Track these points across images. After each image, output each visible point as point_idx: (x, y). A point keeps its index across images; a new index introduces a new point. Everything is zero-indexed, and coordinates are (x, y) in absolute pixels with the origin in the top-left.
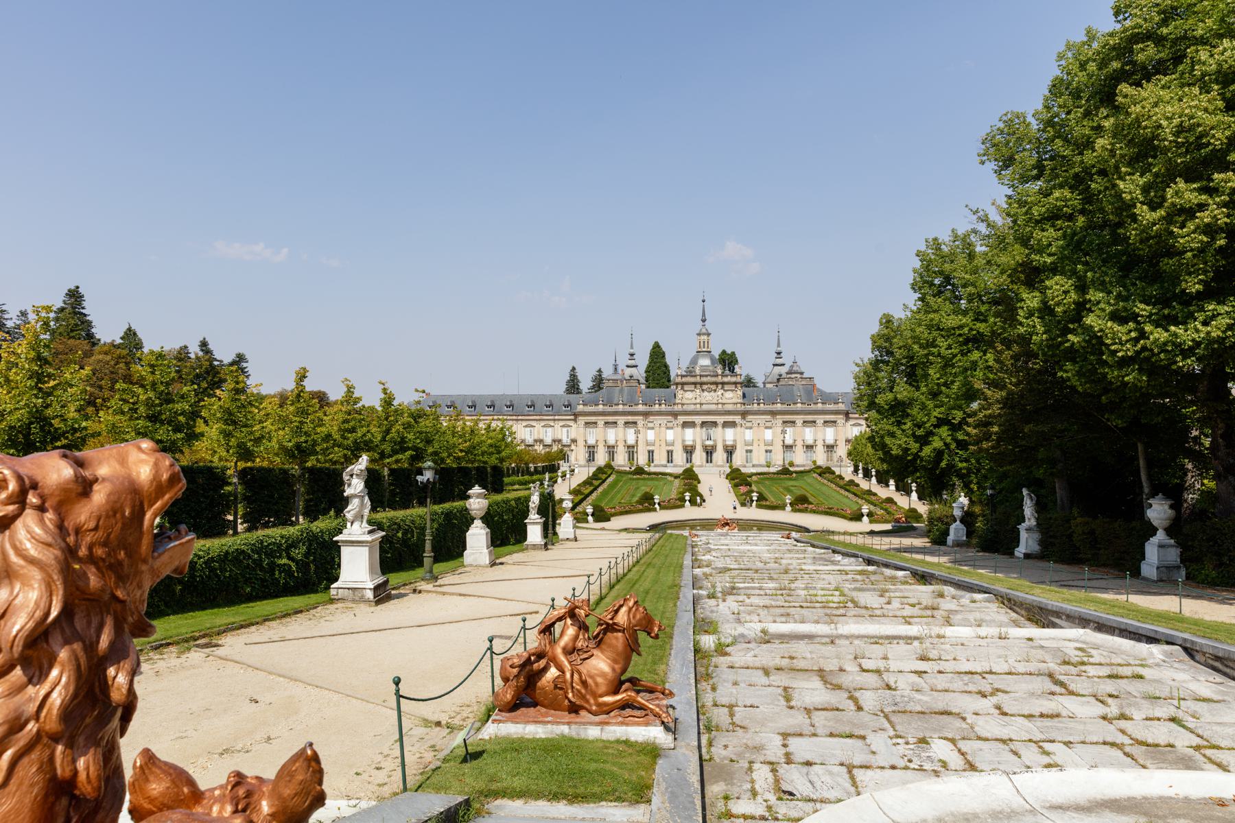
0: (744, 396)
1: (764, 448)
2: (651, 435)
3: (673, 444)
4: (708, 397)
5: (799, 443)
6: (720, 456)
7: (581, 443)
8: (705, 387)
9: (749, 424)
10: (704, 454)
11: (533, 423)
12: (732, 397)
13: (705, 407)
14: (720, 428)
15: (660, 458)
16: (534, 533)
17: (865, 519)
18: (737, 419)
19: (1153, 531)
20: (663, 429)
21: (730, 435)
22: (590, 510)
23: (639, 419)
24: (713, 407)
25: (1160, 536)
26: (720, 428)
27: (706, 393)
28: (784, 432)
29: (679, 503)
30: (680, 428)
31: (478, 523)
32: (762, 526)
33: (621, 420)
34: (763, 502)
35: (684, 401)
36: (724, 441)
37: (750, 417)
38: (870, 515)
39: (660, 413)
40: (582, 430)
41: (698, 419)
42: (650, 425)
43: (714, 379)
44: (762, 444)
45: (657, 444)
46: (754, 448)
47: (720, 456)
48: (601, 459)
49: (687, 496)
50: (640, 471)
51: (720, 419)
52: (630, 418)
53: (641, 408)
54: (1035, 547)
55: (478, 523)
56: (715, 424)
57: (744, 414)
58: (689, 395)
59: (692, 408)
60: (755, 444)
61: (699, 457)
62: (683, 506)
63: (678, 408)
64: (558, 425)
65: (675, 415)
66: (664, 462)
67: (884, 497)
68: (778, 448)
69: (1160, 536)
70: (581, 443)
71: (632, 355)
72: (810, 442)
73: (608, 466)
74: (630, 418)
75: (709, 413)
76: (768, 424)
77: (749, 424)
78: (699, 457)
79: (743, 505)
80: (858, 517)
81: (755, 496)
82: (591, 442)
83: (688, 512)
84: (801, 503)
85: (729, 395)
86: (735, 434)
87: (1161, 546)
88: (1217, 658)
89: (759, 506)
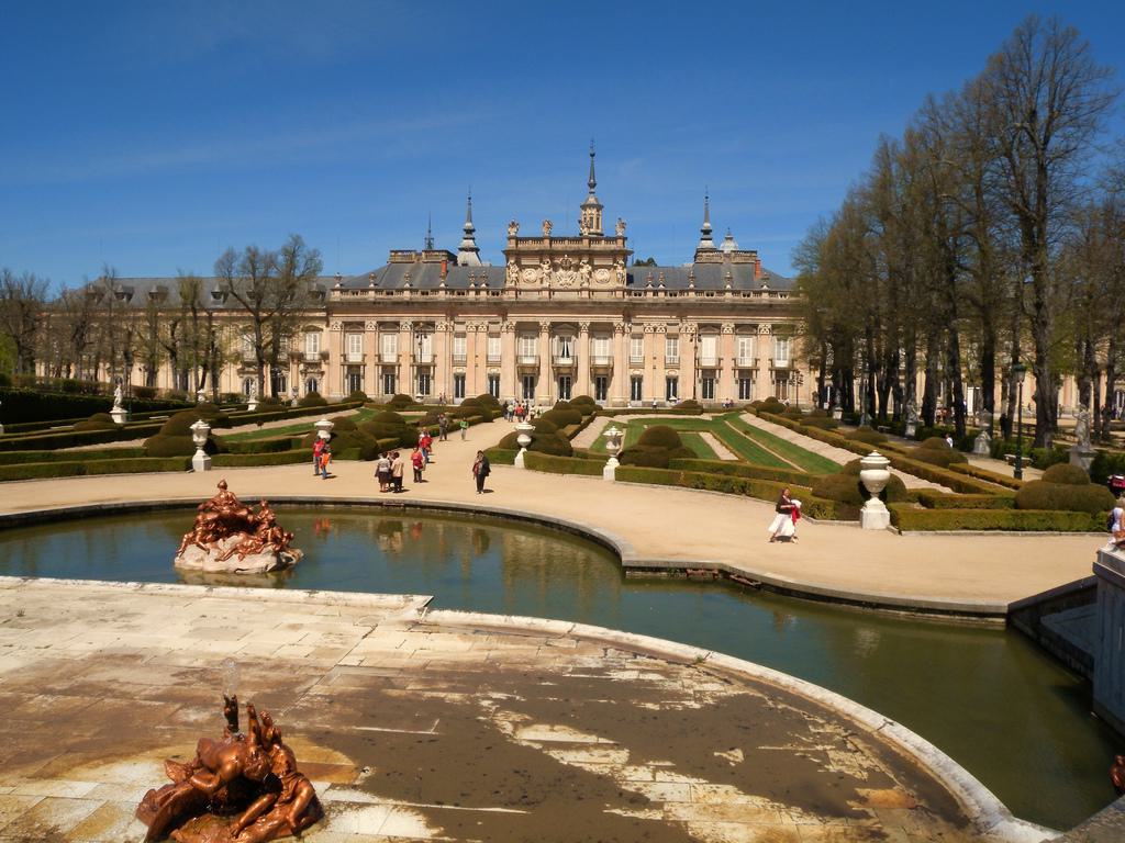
0: (630, 279)
1: (662, 374)
2: (460, 346)
3: (498, 365)
4: (563, 277)
7: (335, 359)
8: (558, 261)
9: (636, 329)
10: (555, 385)
12: (607, 279)
13: (558, 296)
14: (584, 336)
17: (875, 510)
18: (617, 320)
20: (482, 336)
21: (602, 350)
23: (441, 321)
24: (573, 296)
26: (584, 336)
30: (512, 335)
35: (522, 285)
36: (592, 358)
37: (639, 318)
39: (476, 308)
41: (545, 319)
43: (575, 246)
44: (660, 367)
45: (471, 363)
46: (646, 373)
51: (585, 320)
52: (423, 317)
53: (442, 296)
56: (575, 328)
57: (629, 311)
58: (530, 274)
59: (535, 297)
60: (648, 367)
63: (509, 296)
65: (502, 310)
70: (335, 359)
71: (469, 231)
72: (748, 363)
74: (423, 317)
75: (562, 306)
76: (672, 330)
77: (636, 329)
82: (355, 358)
86: (612, 347)
89: (531, 465)
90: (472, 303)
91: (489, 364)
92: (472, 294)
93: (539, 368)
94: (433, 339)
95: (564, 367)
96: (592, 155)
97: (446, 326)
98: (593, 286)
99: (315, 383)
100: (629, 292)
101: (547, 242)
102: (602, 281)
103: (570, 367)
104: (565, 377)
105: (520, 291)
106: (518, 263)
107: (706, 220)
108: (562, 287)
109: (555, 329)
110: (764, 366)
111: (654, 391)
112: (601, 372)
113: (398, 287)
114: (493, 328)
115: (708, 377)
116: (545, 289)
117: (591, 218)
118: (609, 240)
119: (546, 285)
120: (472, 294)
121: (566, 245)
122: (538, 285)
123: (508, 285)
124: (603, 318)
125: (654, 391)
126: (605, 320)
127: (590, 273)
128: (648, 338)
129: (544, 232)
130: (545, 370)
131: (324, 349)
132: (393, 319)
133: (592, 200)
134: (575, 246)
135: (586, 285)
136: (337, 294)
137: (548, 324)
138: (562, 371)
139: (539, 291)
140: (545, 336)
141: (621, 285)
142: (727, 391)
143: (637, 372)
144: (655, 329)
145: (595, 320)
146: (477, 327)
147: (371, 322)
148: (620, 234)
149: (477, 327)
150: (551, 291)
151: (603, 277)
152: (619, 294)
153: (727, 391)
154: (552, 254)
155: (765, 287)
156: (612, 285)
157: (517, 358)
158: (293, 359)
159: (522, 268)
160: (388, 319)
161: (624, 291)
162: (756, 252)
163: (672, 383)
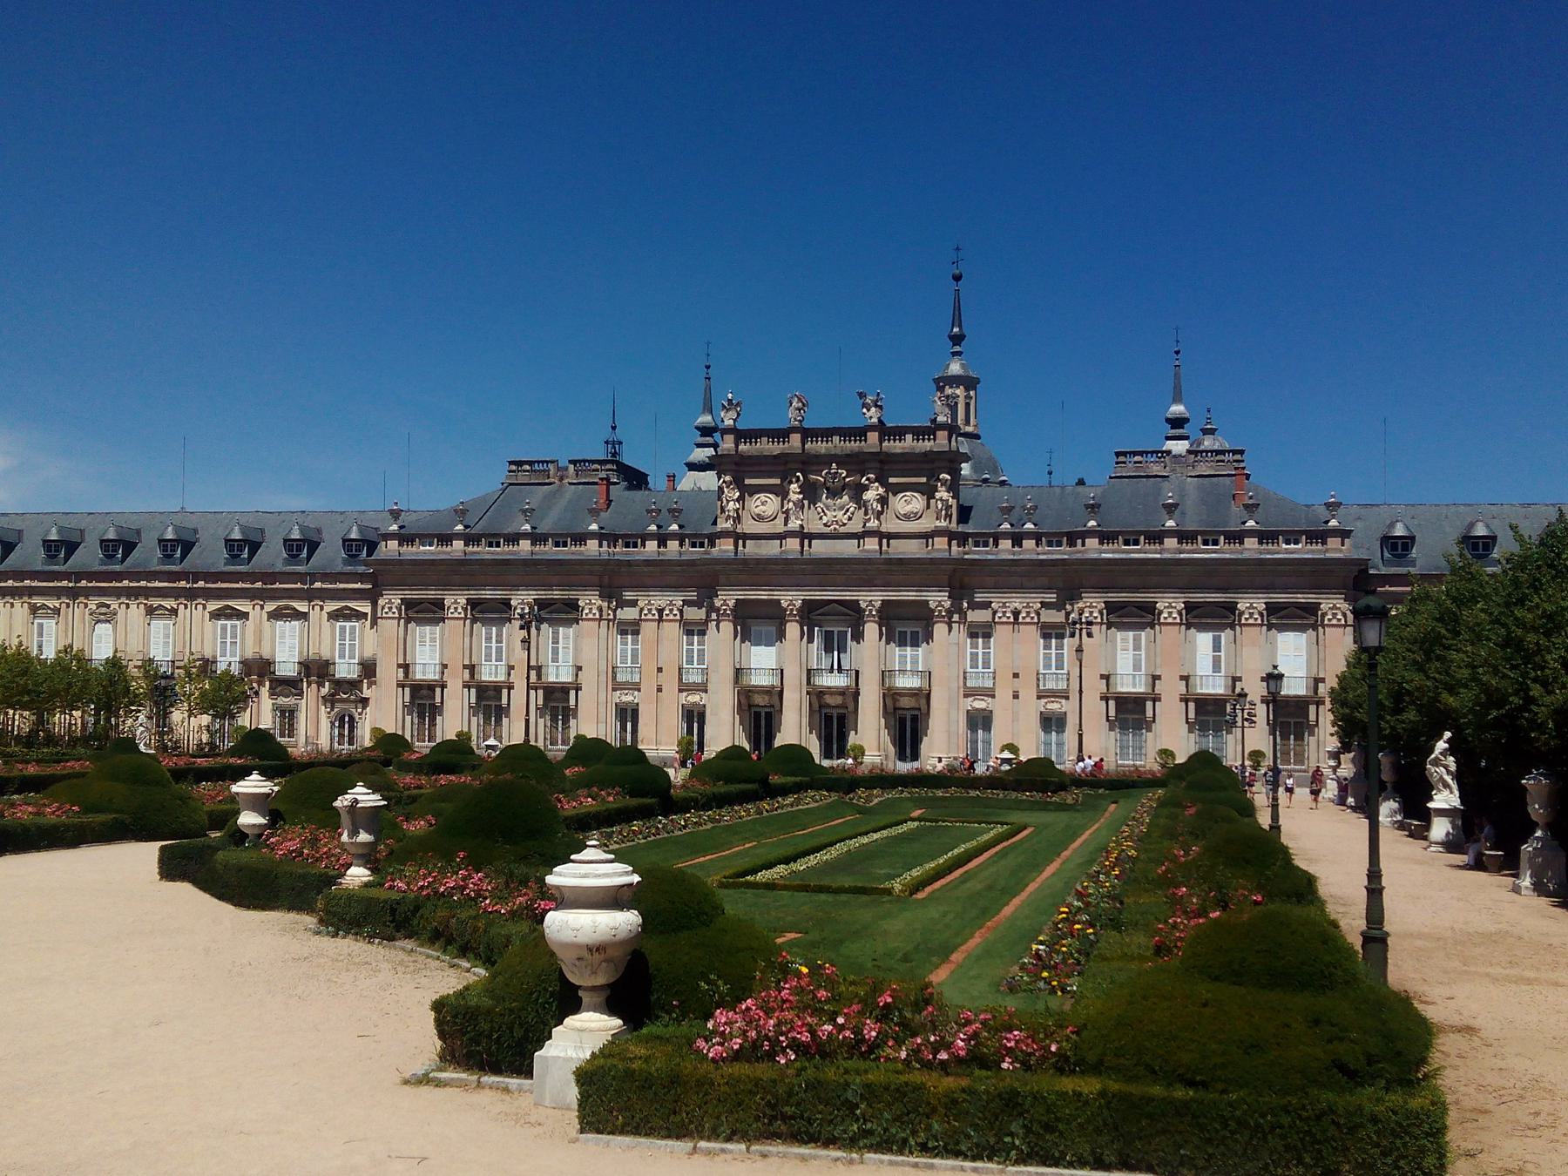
0: (964, 514)
1: (1032, 708)
4: (834, 513)
5: (1171, 690)
7: (388, 673)
11: (242, 605)
13: (820, 548)
20: (672, 630)
30: (727, 627)
35: (749, 526)
40: (390, 627)
44: (1028, 694)
46: (1000, 707)
58: (766, 504)
60: (1003, 694)
64: (319, 614)
70: (388, 673)
72: (1215, 686)
76: (1056, 617)
82: (425, 671)
85: (908, 503)
91: (684, 688)
92: (652, 545)
93: (781, 693)
94: (576, 637)
95: (830, 691)
97: (600, 610)
98: (890, 525)
99: (352, 718)
100: (962, 539)
101: (796, 439)
102: (907, 517)
103: (842, 692)
104: (835, 713)
105: (745, 537)
106: (738, 482)
107: (1177, 399)
108: (827, 530)
109: (810, 614)
112: (905, 702)
113: (509, 530)
116: (792, 534)
118: (919, 433)
119: (794, 524)
120: (652, 545)
121: (837, 445)
122: (778, 526)
123: (724, 525)
127: (883, 501)
128: (1001, 633)
129: (792, 417)
131: (368, 654)
133: (955, 368)
134: (853, 446)
135: (873, 524)
136: (393, 544)
137: (798, 603)
138: (829, 700)
139: (781, 537)
140: (793, 629)
141: (943, 524)
144: (1016, 613)
145: (893, 596)
146: (660, 611)
147: (455, 601)
148: (941, 419)
149: (660, 611)
150: (804, 536)
151: (909, 508)
152: (940, 543)
154: (809, 462)
155: (1251, 523)
156: (927, 524)
157: (738, 673)
158: (308, 676)
161: (951, 536)
162: (1241, 452)
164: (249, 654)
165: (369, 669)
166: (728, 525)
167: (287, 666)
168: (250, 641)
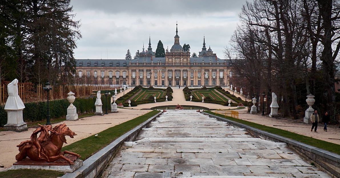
1: (197, 79)
4: (178, 61)
6: (182, 82)
15: (160, 83)
16: (99, 110)
17: (229, 105)
18: (188, 69)
19: (308, 107)
22: (130, 102)
25: (310, 109)
27: (176, 59)
28: (205, 74)
29: (162, 100)
31: (72, 105)
32: (194, 107)
33: (145, 69)
34: (195, 100)
38: (231, 103)
41: (174, 69)
42: (156, 71)
45: (158, 78)
47: (182, 82)
48: (138, 84)
49: (167, 97)
50: (151, 88)
51: (182, 69)
52: (148, 68)
54: (276, 113)
55: (72, 105)
60: (195, 78)
61: (174, 82)
62: (165, 101)
66: (161, 85)
67: (237, 97)
68: (203, 80)
69: (310, 109)
70: (130, 77)
72: (214, 77)
73: (140, 86)
74: (148, 68)
78: (174, 82)
79: (187, 100)
80: (227, 105)
81: (191, 97)
83: (167, 103)
84: (208, 100)
87: (310, 112)
88: (294, 146)
90: (158, 66)
96: (177, 25)
110: (218, 78)
111: (196, 83)
114: (163, 71)
115: (207, 80)
117: (177, 40)
119: (174, 62)
124: (185, 68)
125: (196, 83)
126: (186, 69)
130: (174, 79)
132: (142, 69)
135: (182, 62)
142: (210, 83)
143: (192, 80)
153: (210, 83)
157: (168, 77)
159: (169, 59)
160: (141, 69)
163: (200, 84)
164: (113, 75)
165: (127, 77)
166: (167, 62)
167: (118, 77)
168: (113, 74)
